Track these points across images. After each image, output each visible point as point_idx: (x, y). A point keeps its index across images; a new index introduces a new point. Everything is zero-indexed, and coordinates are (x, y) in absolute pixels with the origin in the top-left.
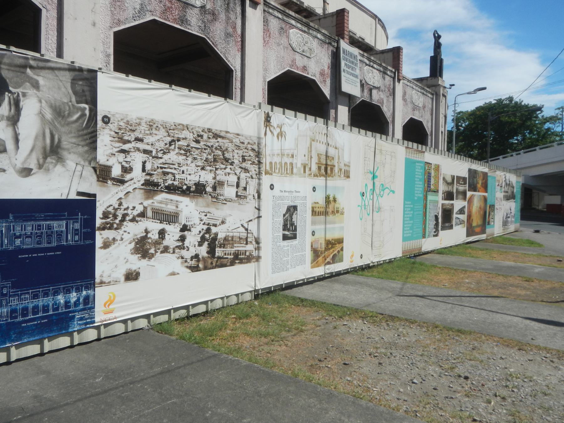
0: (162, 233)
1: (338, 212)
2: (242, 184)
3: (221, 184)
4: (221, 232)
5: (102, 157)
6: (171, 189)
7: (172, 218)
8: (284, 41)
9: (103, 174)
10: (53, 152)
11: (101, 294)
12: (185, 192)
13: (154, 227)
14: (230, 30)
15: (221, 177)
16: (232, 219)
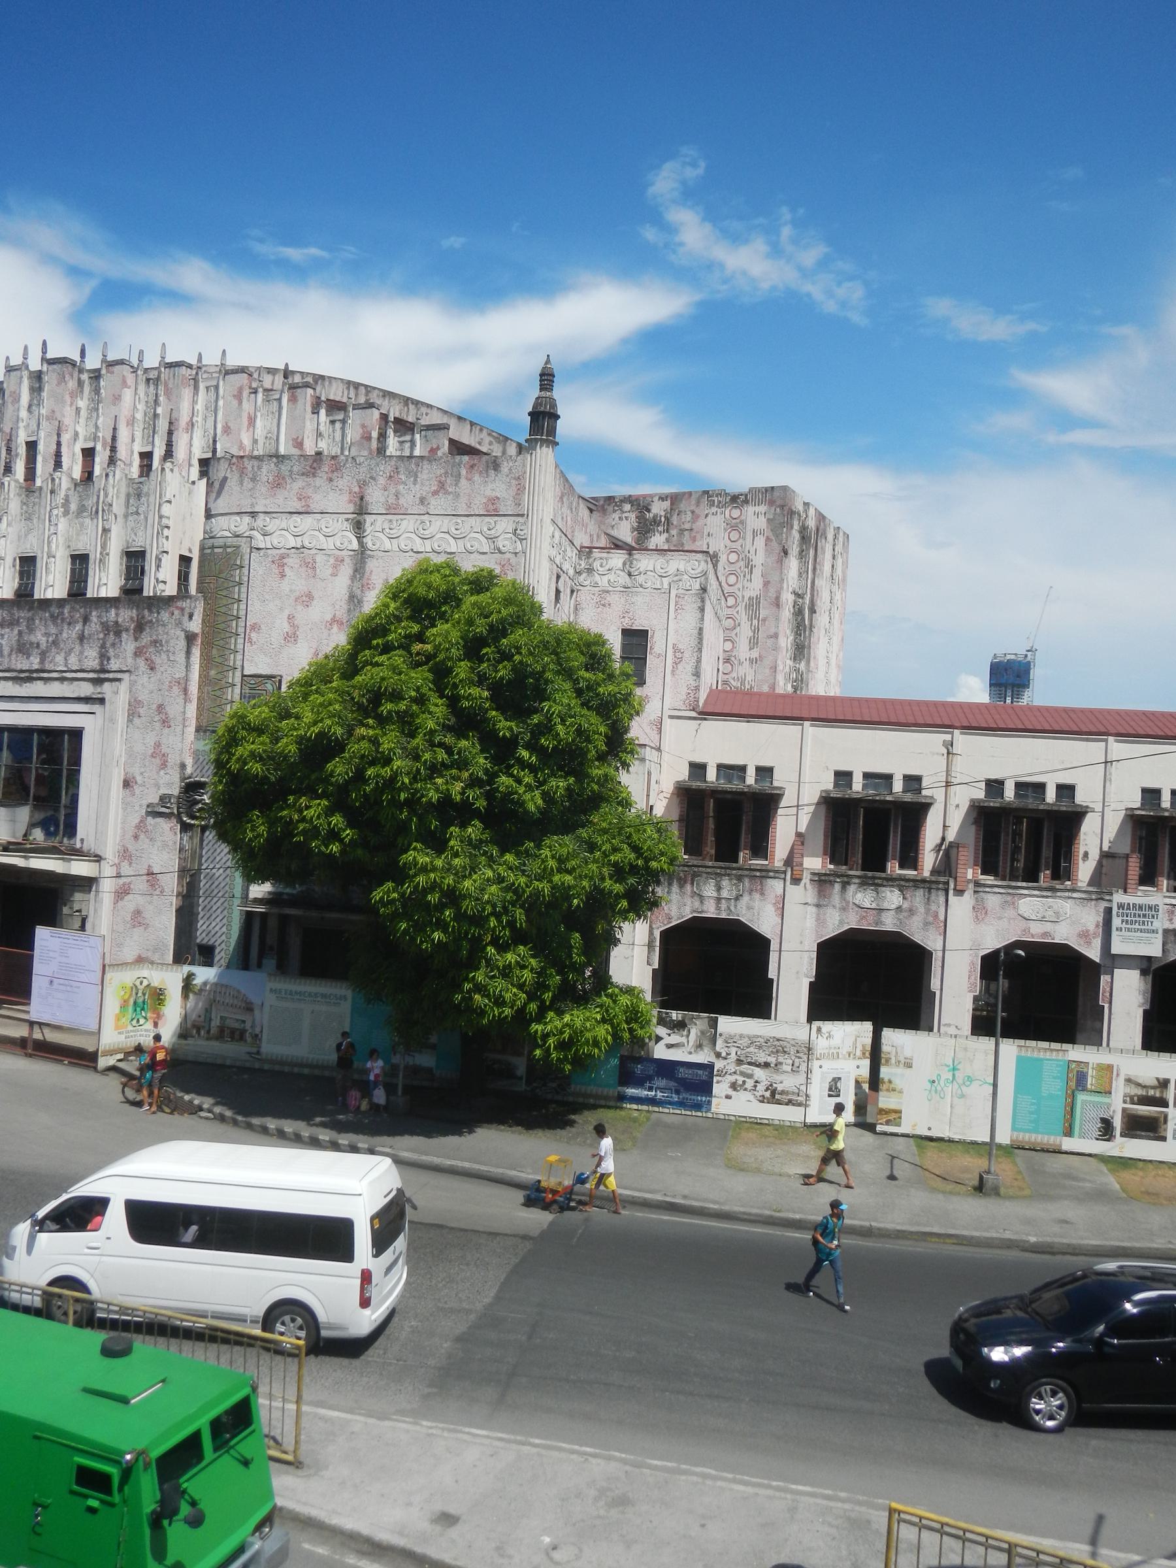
0: (744, 1082)
1: (894, 1090)
2: (796, 1064)
3: (781, 1063)
4: (780, 1088)
5: (718, 1049)
6: (750, 1064)
7: (750, 1076)
8: (1010, 912)
9: (718, 1055)
10: (700, 1046)
11: (714, 1101)
12: (759, 1066)
13: (740, 1079)
14: (931, 919)
15: (781, 1059)
16: (787, 1082)
